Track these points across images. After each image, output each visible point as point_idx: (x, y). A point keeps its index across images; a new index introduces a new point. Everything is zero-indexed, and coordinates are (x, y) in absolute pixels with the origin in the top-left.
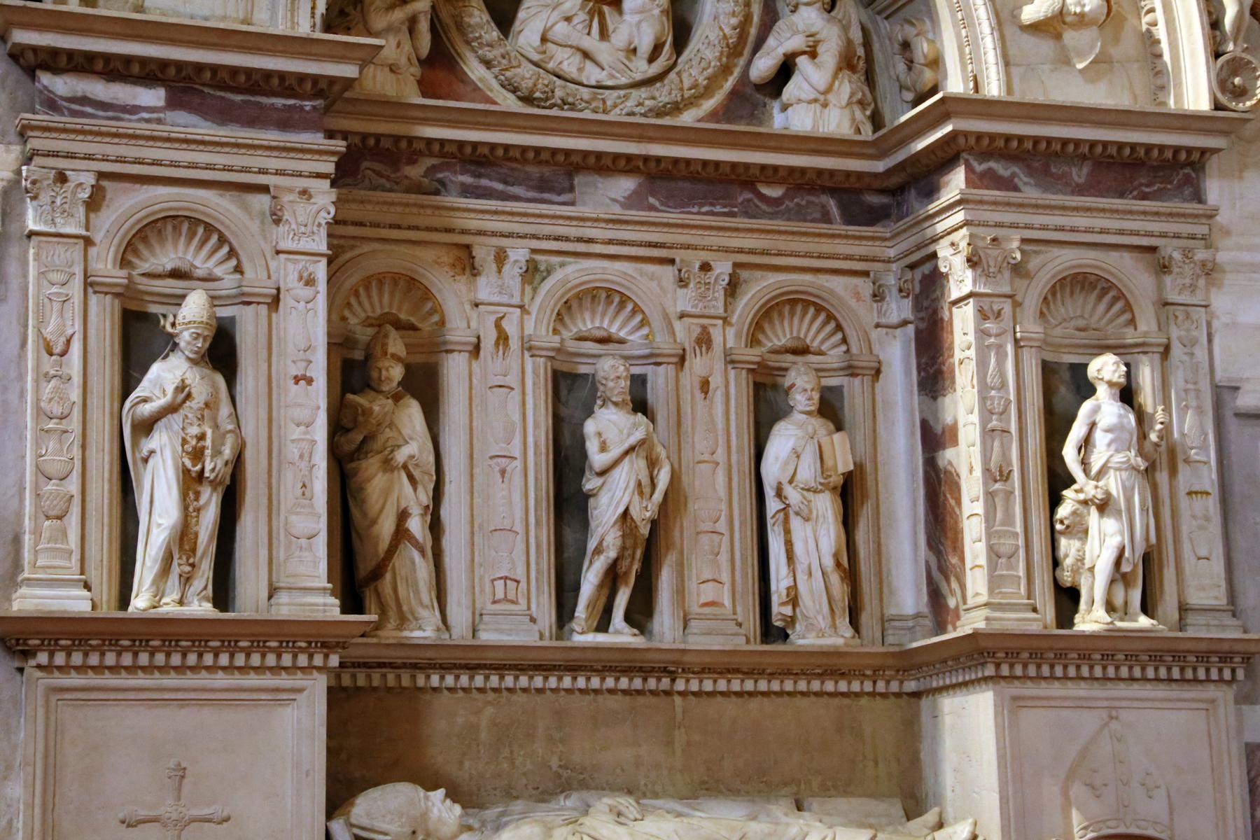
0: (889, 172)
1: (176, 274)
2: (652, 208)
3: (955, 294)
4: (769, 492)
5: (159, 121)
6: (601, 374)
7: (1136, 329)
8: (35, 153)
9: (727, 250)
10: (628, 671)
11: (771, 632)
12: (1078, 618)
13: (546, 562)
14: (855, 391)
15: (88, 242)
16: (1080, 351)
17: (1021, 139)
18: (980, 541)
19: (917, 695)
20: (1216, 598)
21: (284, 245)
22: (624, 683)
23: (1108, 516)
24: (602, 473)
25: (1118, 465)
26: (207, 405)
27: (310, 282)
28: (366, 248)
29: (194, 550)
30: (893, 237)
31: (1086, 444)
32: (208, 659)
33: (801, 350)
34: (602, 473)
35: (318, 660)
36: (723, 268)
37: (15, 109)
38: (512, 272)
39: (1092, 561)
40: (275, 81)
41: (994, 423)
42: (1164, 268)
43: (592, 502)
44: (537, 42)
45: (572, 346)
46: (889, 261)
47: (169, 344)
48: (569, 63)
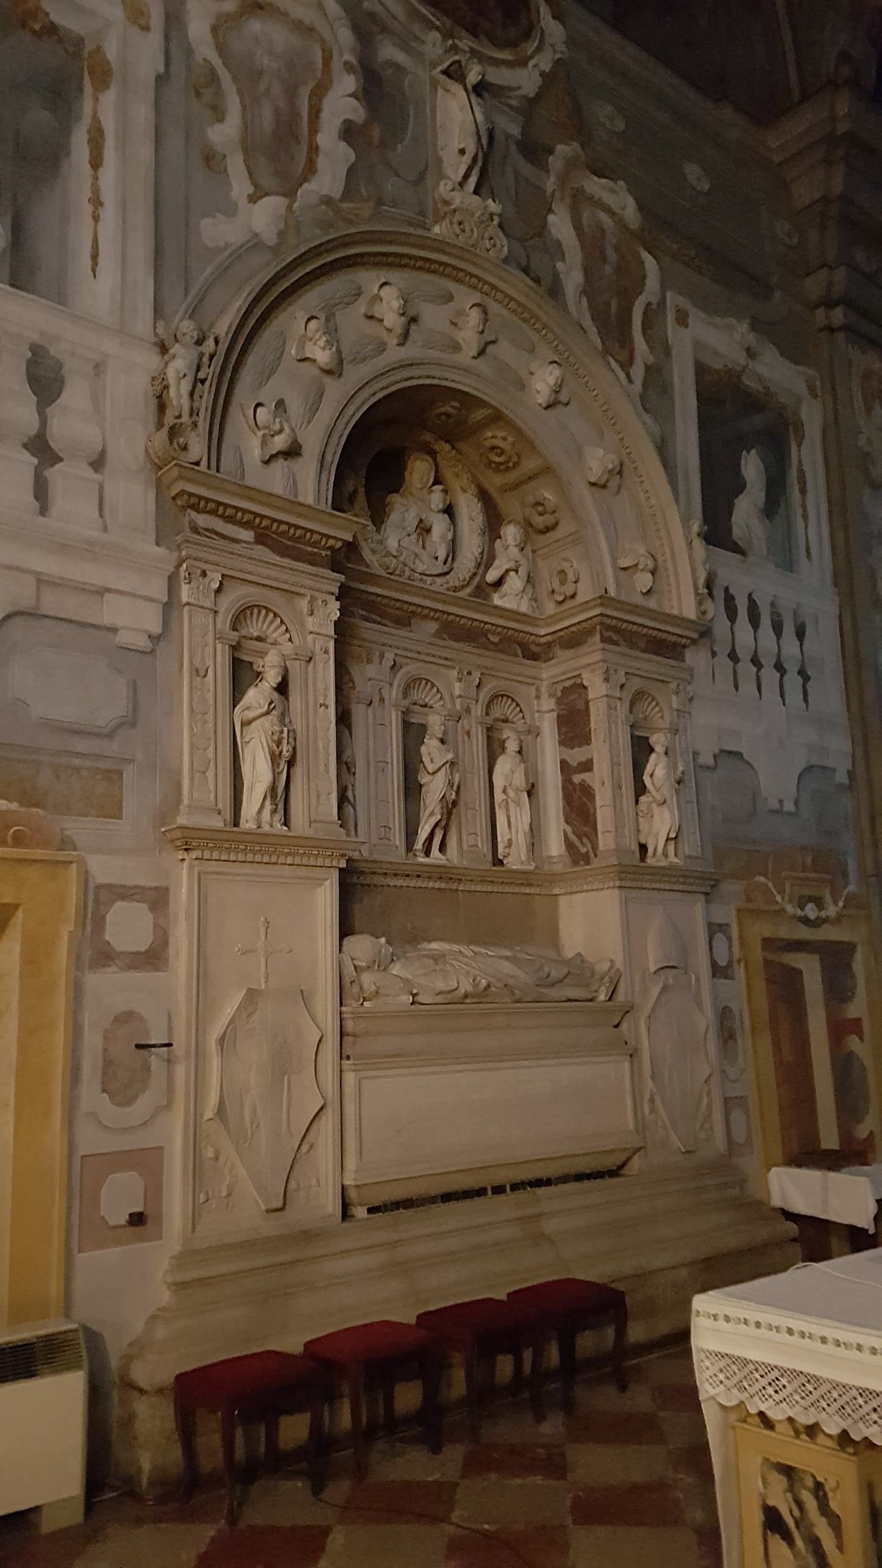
33: (506, 721)
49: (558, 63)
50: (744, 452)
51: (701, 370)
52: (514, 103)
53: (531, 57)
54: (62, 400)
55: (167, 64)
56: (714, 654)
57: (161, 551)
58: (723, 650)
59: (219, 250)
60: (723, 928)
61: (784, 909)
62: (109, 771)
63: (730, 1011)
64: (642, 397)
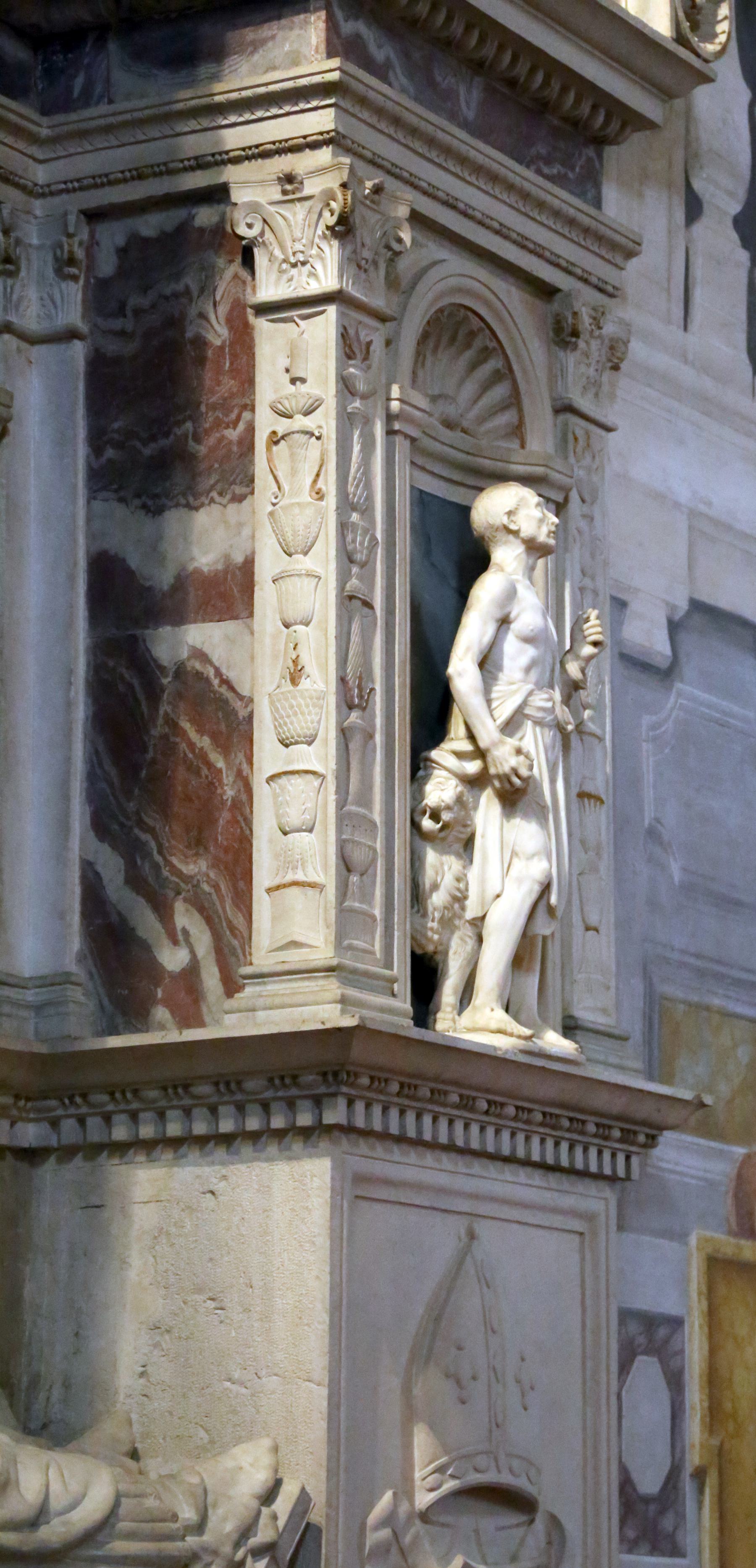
7: (523, 446)
16: (437, 469)
18: (310, 830)
20: (604, 1011)
23: (526, 816)
25: (540, 714)
30: (54, 140)
39: (483, 903)
41: (354, 583)
46: (31, 191)
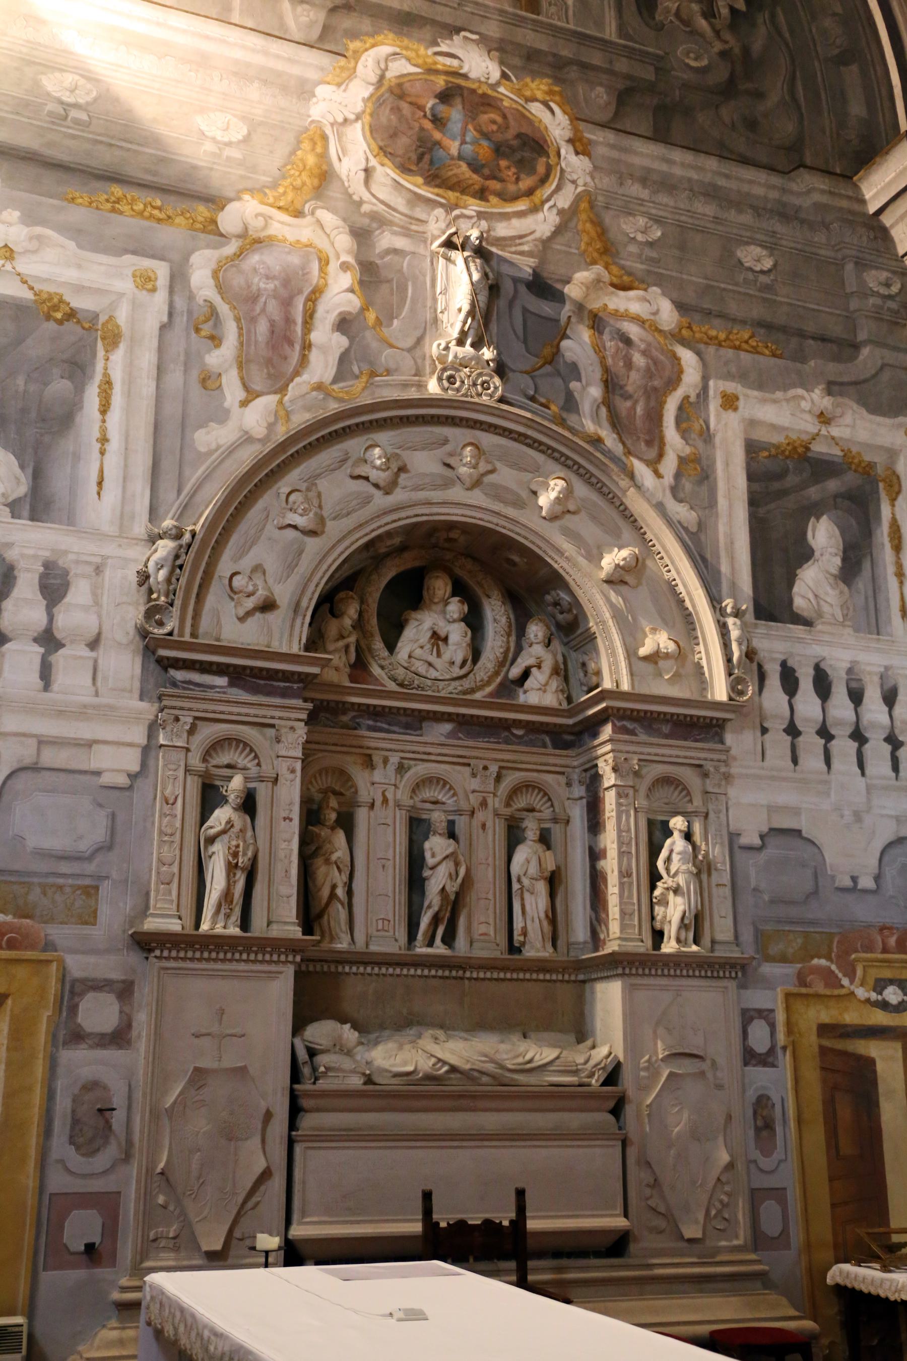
0: (575, 725)
1: (229, 766)
2: (460, 739)
3: (606, 785)
4: (514, 880)
5: (224, 693)
6: (433, 819)
8: (165, 707)
9: (496, 760)
10: (442, 967)
11: (513, 949)
12: (663, 946)
13: (403, 911)
14: (557, 831)
15: (188, 750)
17: (638, 711)
19: (584, 982)
21: (281, 754)
22: (440, 973)
24: (432, 868)
26: (241, 830)
27: (293, 771)
28: (320, 755)
29: (232, 902)
31: (668, 860)
32: (237, 956)
33: (532, 810)
34: (432, 868)
35: (290, 958)
36: (494, 769)
37: (157, 686)
38: (391, 768)
40: (280, 675)
41: (624, 849)
42: (706, 775)
43: (427, 882)
44: (406, 657)
45: (420, 805)
47: (224, 800)
48: (422, 668)
49: (578, 199)
50: (813, 519)
51: (752, 448)
52: (526, 248)
53: (548, 200)
54: (68, 599)
55: (170, 314)
56: (764, 731)
57: (144, 705)
58: (777, 727)
59: (210, 453)
60: (766, 1015)
61: (853, 993)
62: (87, 887)
63: (768, 1098)
64: (675, 491)
